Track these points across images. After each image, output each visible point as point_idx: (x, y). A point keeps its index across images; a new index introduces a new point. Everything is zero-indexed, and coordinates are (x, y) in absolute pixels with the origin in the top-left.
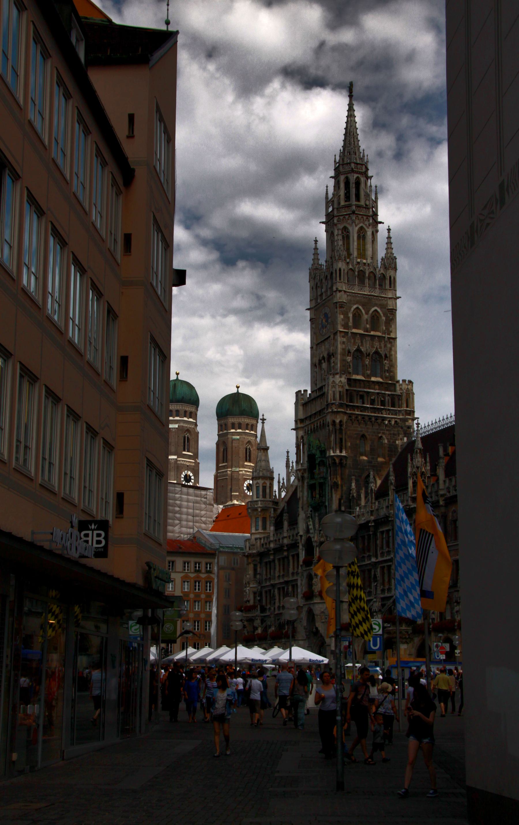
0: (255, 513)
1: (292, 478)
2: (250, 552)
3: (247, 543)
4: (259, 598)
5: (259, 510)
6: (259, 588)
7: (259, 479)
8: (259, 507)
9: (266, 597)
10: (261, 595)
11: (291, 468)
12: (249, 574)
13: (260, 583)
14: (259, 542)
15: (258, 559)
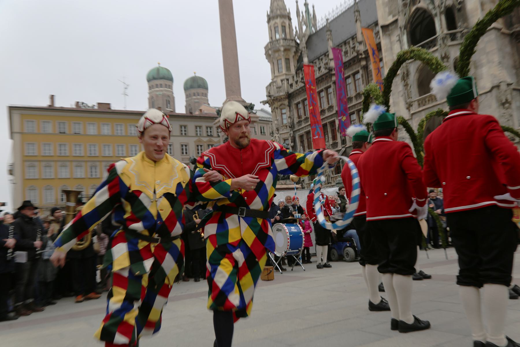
0: (277, 55)
1: (304, 28)
2: (277, 95)
3: (272, 86)
4: (292, 144)
5: (282, 49)
6: (292, 132)
7: (277, 17)
8: (283, 46)
9: (302, 142)
10: (294, 140)
11: (301, 18)
12: (277, 120)
13: (292, 126)
14: (285, 82)
15: (286, 102)
